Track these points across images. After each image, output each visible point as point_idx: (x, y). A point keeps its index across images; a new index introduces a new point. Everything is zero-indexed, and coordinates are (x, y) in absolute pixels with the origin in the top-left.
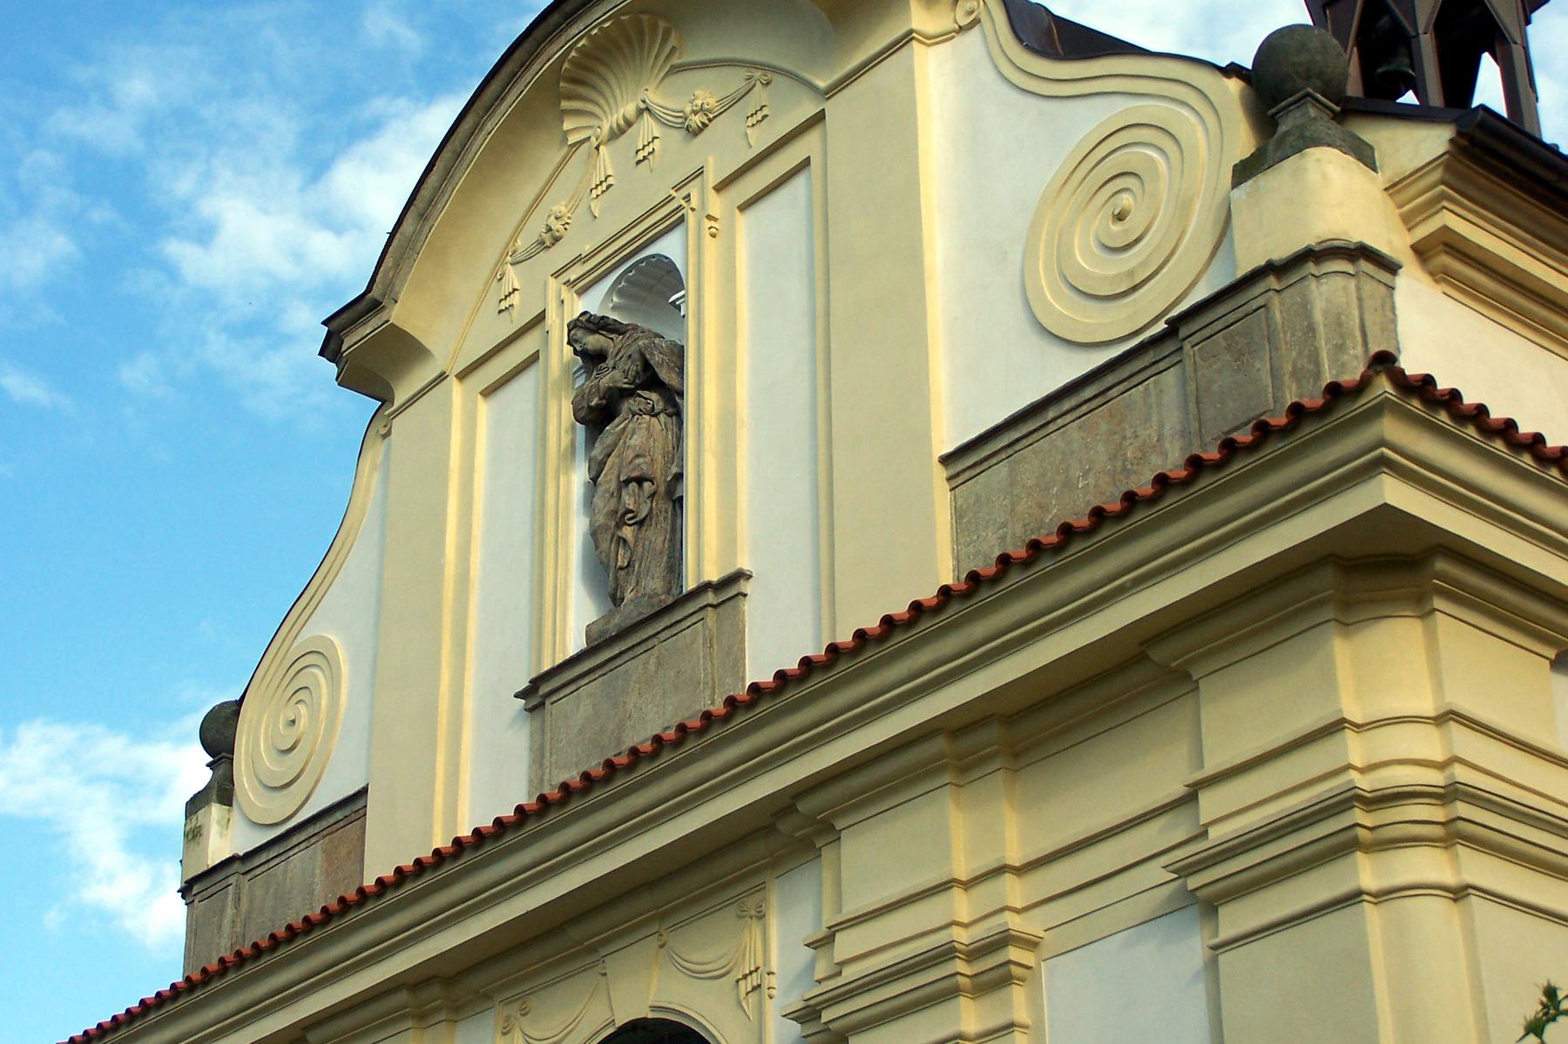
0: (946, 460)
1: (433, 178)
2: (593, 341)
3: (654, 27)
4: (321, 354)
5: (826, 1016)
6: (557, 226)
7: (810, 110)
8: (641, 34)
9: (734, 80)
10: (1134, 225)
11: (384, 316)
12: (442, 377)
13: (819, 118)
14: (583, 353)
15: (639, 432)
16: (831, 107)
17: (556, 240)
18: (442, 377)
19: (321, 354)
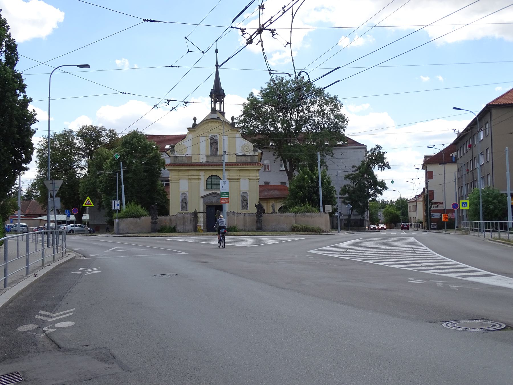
15: (214, 145)
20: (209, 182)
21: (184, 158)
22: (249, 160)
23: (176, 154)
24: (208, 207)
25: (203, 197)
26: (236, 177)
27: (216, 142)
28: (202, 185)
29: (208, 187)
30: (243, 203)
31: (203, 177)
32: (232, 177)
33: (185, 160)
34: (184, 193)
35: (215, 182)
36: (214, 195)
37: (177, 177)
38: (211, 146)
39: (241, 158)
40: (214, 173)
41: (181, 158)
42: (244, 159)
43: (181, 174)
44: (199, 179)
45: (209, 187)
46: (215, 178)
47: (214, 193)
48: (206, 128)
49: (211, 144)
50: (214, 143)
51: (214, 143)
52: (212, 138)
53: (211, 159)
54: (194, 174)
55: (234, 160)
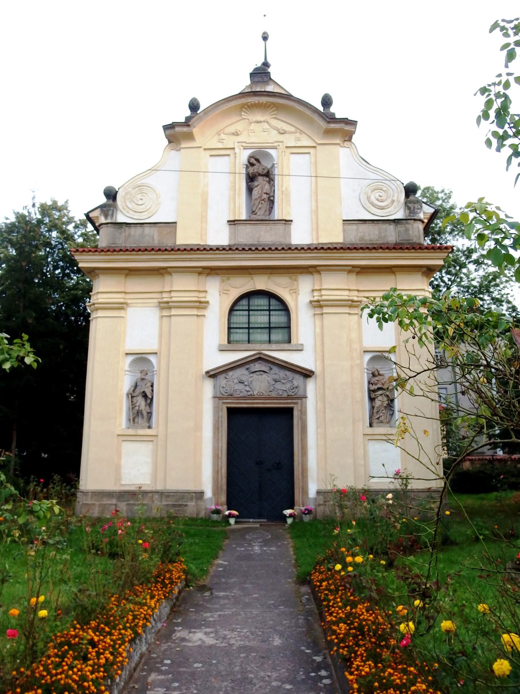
0: (344, 220)
1: (210, 108)
2: (253, 161)
3: (272, 108)
4: (166, 128)
5: (321, 303)
6: (239, 133)
7: (314, 145)
8: (269, 107)
9: (293, 129)
10: (384, 198)
11: (190, 129)
12: (200, 147)
13: (315, 147)
14: (249, 162)
16: (318, 147)
17: (238, 135)
18: (200, 147)
19: (166, 128)
20: (240, 319)
21: (147, 230)
22: (391, 235)
23: (121, 218)
24: (232, 412)
25: (213, 375)
26: (344, 295)
27: (268, 175)
28: (213, 324)
29: (234, 337)
30: (372, 400)
31: (218, 296)
32: (327, 295)
33: (154, 237)
34: (141, 359)
35: (261, 319)
36: (257, 366)
37: (118, 298)
38: (250, 190)
39: (363, 227)
40: (261, 283)
41: (139, 230)
42: (371, 234)
43: (135, 285)
44: (202, 305)
45: (241, 335)
46: (262, 302)
47: (260, 359)
48: (232, 129)
49: (251, 178)
50: (259, 175)
51: (259, 175)
52: (254, 161)
53: (248, 235)
54: (182, 286)
55: (335, 236)
